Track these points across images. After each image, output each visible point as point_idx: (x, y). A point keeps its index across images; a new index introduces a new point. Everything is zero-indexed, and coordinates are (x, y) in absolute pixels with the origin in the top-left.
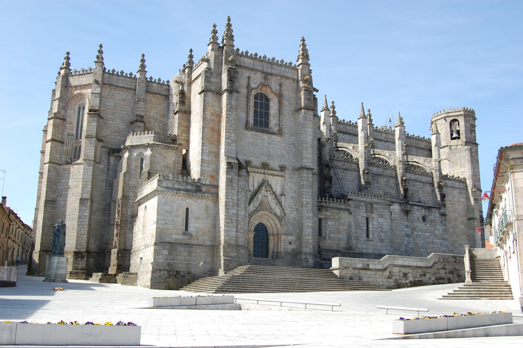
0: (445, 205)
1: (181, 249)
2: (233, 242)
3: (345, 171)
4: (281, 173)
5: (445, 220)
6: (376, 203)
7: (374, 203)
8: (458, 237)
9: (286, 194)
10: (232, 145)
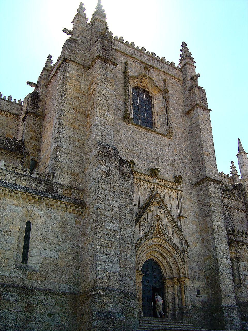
1: (11, 296)
2: (114, 285)
10: (108, 126)
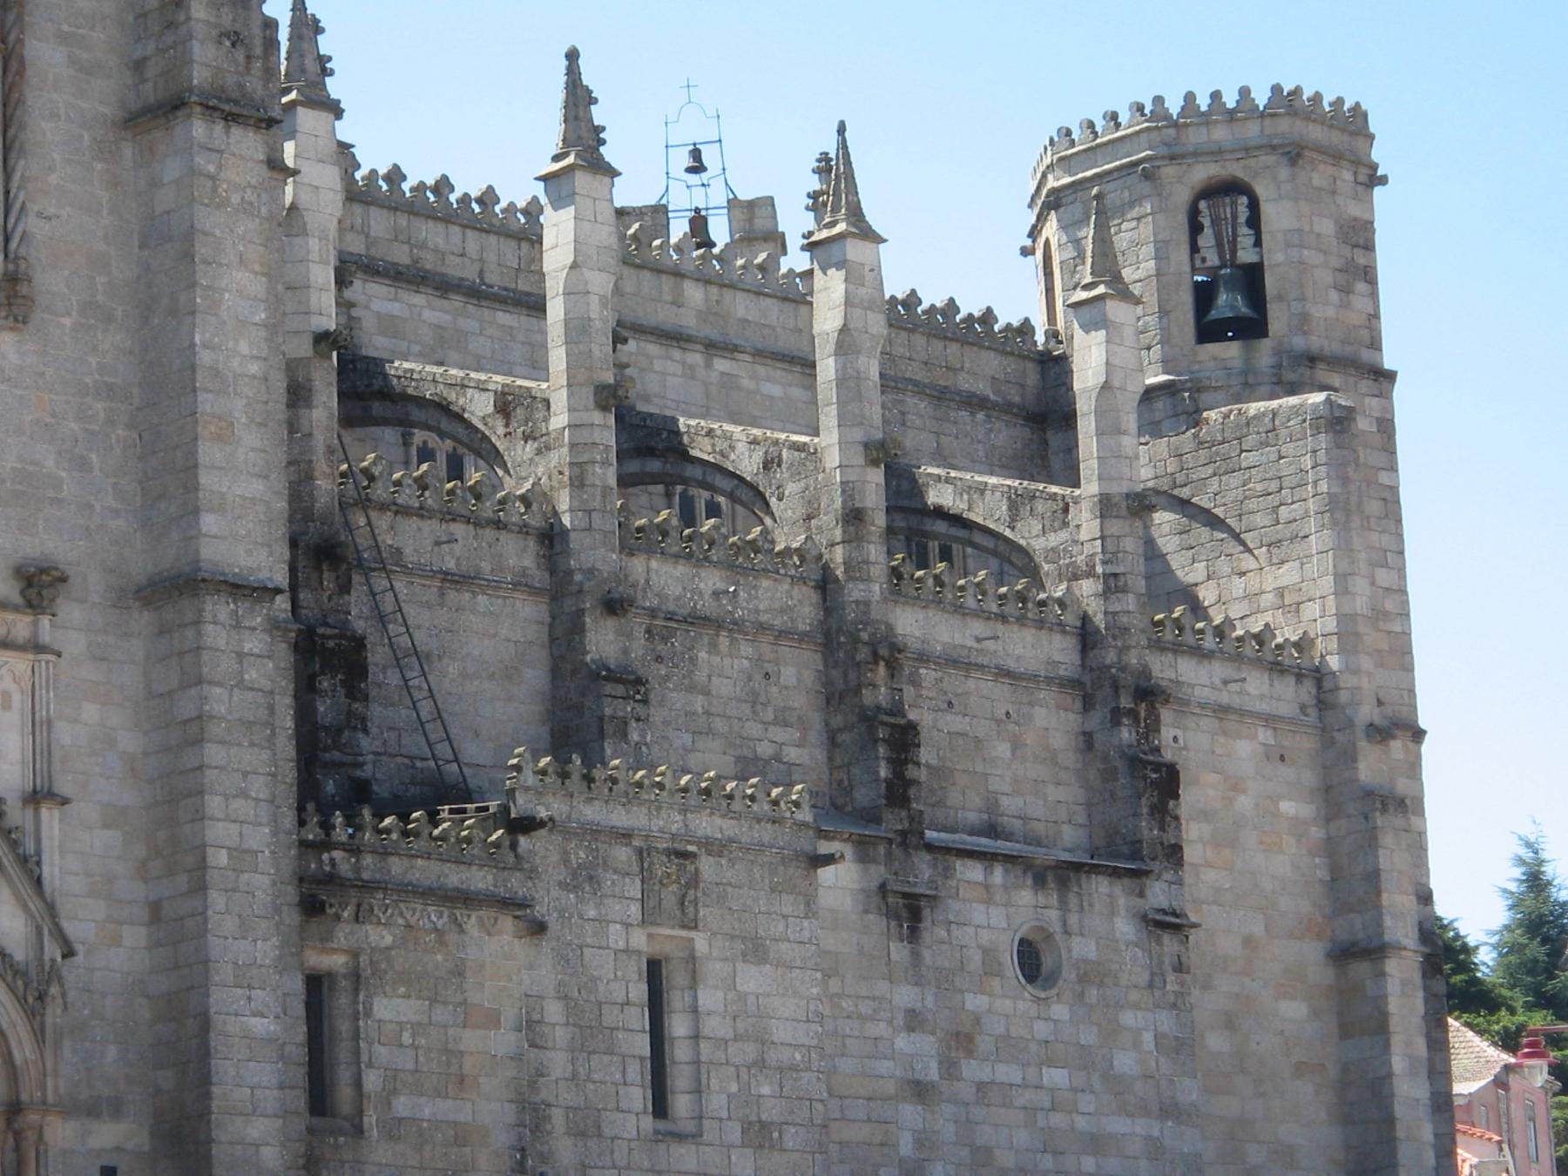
0: (1174, 853)
3: (452, 595)
4: (29, 619)
5: (1180, 968)
6: (717, 847)
7: (698, 844)
8: (1263, 1095)
9: (64, 786)
